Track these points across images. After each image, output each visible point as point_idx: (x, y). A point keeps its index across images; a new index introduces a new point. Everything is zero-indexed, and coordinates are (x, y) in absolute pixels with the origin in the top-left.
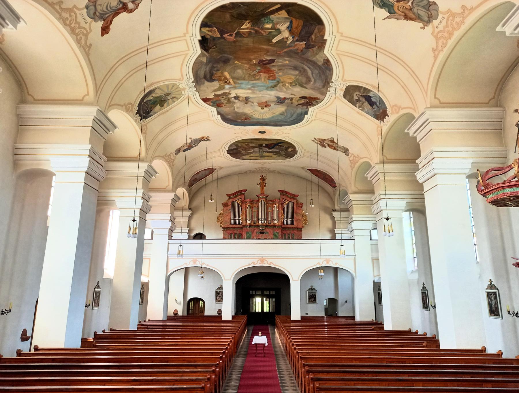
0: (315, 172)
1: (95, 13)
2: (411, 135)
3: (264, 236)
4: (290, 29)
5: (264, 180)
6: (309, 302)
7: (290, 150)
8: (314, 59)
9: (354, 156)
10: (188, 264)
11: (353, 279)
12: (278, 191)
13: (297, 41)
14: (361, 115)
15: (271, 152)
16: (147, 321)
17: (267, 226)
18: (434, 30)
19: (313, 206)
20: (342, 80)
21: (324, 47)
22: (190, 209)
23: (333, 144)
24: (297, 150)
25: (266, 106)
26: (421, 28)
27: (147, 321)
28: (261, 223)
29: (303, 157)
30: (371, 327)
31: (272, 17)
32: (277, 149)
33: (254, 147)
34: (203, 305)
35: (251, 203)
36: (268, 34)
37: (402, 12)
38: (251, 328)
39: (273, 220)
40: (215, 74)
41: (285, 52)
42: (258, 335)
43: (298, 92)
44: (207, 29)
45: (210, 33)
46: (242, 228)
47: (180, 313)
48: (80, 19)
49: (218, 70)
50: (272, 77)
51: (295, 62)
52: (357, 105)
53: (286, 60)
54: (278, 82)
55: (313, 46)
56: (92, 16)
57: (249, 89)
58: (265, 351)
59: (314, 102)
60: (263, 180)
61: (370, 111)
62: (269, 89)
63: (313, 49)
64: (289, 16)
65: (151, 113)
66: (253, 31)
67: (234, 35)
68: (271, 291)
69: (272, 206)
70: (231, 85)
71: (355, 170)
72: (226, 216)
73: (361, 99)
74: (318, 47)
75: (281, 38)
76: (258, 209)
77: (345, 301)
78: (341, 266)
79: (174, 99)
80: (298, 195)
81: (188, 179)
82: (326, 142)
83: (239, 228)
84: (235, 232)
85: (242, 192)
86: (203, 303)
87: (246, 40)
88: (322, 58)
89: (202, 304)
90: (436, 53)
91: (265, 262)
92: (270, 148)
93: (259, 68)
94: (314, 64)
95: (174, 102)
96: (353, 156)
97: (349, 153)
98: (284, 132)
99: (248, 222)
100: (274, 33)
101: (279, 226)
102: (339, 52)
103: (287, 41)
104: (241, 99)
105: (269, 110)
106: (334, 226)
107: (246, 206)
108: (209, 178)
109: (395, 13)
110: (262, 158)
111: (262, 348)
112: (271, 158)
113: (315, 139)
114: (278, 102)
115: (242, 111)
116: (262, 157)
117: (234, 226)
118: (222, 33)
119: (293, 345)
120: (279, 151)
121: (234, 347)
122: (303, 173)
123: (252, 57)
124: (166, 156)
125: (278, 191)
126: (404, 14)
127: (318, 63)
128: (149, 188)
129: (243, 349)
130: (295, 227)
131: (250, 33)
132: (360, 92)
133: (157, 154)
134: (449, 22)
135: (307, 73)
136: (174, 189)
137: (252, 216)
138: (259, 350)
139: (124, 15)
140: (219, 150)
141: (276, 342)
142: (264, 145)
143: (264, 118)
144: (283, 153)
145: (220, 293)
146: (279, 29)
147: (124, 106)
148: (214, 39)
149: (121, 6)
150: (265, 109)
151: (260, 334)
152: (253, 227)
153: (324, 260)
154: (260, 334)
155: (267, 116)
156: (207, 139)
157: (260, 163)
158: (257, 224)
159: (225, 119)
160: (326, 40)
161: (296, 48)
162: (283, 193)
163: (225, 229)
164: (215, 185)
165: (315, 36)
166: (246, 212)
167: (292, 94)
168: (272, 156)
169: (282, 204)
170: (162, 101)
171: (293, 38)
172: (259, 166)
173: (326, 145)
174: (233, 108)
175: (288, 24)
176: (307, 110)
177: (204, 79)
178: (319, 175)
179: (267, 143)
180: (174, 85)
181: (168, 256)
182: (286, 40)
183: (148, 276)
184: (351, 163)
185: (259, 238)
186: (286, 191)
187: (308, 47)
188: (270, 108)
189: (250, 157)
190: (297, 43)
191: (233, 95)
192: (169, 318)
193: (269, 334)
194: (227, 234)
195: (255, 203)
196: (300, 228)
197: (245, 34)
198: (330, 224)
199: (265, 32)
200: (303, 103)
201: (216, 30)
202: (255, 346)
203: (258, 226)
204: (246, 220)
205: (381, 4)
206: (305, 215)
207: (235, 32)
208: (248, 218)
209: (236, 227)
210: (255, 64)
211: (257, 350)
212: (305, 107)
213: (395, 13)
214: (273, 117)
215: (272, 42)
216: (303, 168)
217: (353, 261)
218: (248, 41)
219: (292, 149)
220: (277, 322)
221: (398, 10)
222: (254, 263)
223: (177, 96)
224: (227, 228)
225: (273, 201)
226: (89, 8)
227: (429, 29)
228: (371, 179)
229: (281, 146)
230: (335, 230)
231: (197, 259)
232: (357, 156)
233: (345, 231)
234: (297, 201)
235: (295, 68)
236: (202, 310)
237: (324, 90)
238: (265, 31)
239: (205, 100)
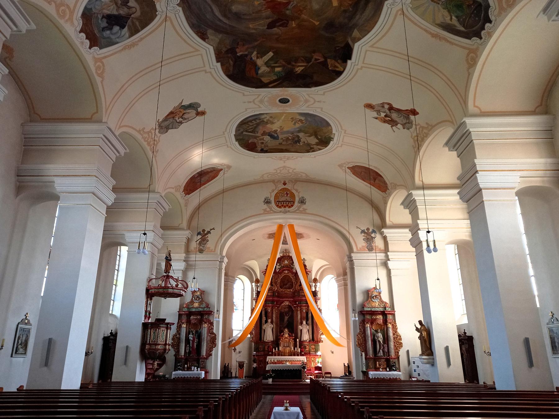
4: (256, 68)
8: (220, 36)
13: (246, 55)
21: (215, 54)
31: (275, 78)
36: (278, 61)
37: (176, 112)
41: (257, 41)
44: (337, 69)
45: (337, 64)
53: (254, 29)
55: (227, 52)
63: (227, 49)
66: (294, 64)
67: (313, 60)
74: (222, 52)
75: (264, 58)
88: (212, 40)
100: (271, 62)
103: (257, 54)
118: (325, 64)
126: (174, 112)
127: (214, 32)
131: (296, 61)
139: (395, 106)
146: (268, 67)
148: (335, 58)
165: (230, 64)
171: (251, 58)
175: (260, 72)
182: (259, 55)
187: (232, 51)
190: (246, 53)
197: (302, 60)
199: (281, 63)
201: (329, 66)
205: (192, 105)
207: (311, 63)
215: (273, 52)
221: (180, 111)
235: (238, 16)
238: (280, 65)
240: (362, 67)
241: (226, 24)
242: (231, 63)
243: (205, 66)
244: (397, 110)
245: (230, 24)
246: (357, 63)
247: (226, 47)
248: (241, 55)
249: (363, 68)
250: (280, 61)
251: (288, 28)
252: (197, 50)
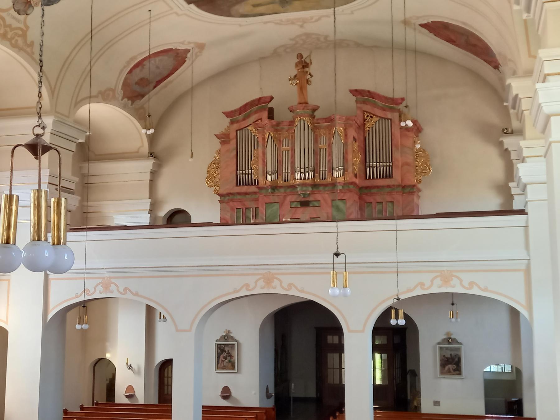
17: (315, 186)
28: (305, 179)
35: (276, 130)
60: (304, 67)
68: (336, 344)
69: (330, 133)
84: (246, 203)
101: (346, 184)
107: (264, 139)
137: (278, 163)
152: (282, 190)
158: (292, 182)
166: (264, 154)
169: (362, 127)
186: (369, 91)
195: (286, 128)
196: (409, 186)
203: (294, 187)
204: (265, 174)
224: (228, 194)
225: (330, 120)
230: (511, 184)
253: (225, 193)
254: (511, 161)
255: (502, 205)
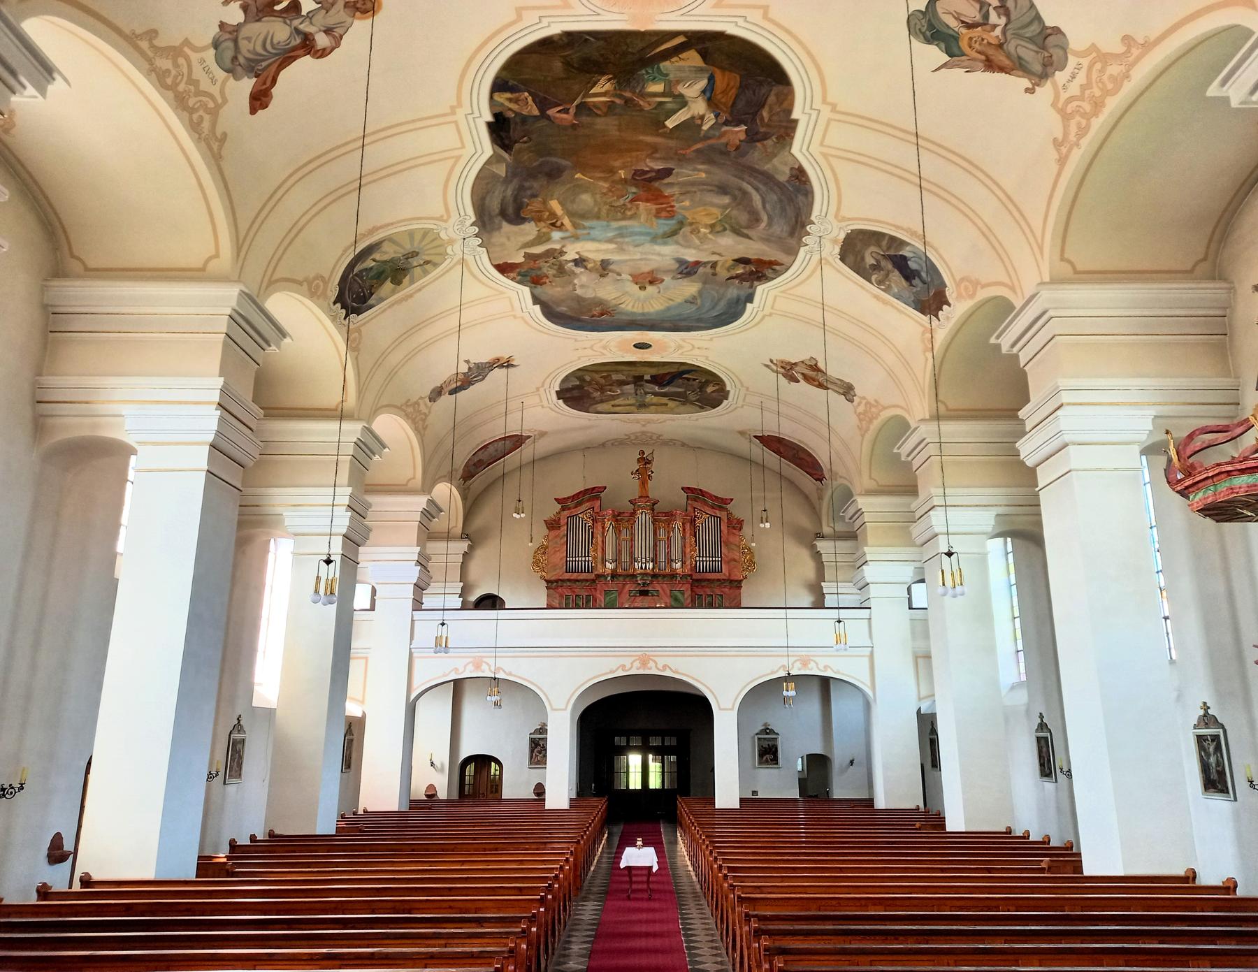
0: (773, 443)
1: (235, 58)
2: (1005, 349)
3: (647, 600)
4: (709, 93)
5: (649, 462)
6: (760, 763)
7: (710, 389)
8: (767, 167)
9: (868, 403)
10: (461, 671)
11: (868, 706)
12: (682, 489)
13: (726, 123)
14: (885, 302)
15: (664, 395)
16: (360, 812)
17: (655, 576)
18: (1057, 96)
19: (768, 525)
20: (836, 216)
21: (792, 138)
22: (465, 535)
23: (815, 373)
24: (728, 388)
25: (651, 283)
26: (1027, 90)
27: (360, 812)
28: (642, 568)
29: (742, 407)
30: (914, 825)
31: (665, 65)
32: (679, 387)
33: (621, 383)
34: (498, 773)
35: (617, 520)
36: (655, 108)
38: (618, 829)
39: (670, 561)
40: (528, 205)
42: (634, 844)
43: (729, 246)
44: (508, 95)
45: (512, 106)
46: (593, 581)
47: (442, 794)
48: (198, 73)
49: (534, 196)
50: (665, 209)
51: (720, 175)
52: (874, 278)
53: (699, 170)
54: (681, 224)
55: (766, 137)
56: (228, 63)
57: (610, 241)
58: (651, 886)
59: (769, 273)
61: (906, 294)
62: (659, 241)
63: (765, 142)
64: (706, 64)
65: (371, 301)
66: (618, 101)
67: (573, 111)
70: (567, 230)
71: (869, 436)
72: (556, 552)
73: (883, 263)
74: (777, 138)
75: (688, 116)
76: (633, 535)
77: (848, 762)
78: (838, 672)
79: (427, 267)
80: (732, 500)
81: (461, 461)
82: (797, 369)
83: (587, 580)
84: (575, 590)
85: (593, 494)
86: (498, 768)
87: (601, 123)
89: (496, 770)
90: (1064, 150)
91: (651, 664)
92: (661, 385)
93: (634, 190)
94: (768, 179)
95: (426, 273)
96: (864, 402)
97: (855, 395)
98: (696, 346)
99: (609, 566)
100: (669, 106)
101: (684, 576)
102: (825, 150)
104: (590, 266)
105: (659, 292)
106: (821, 576)
107: (603, 528)
108: (513, 458)
109: (963, 54)
110: (643, 410)
111: (645, 879)
112: (664, 408)
113: (771, 361)
114: (681, 273)
115: (593, 296)
116: (642, 406)
117: (575, 576)
118: (543, 104)
119: (720, 867)
120: (685, 392)
121: (575, 876)
122: (743, 446)
123: (617, 164)
124: (407, 406)
125: (682, 489)
126: (983, 57)
128: (366, 485)
129: (598, 882)
130: (724, 578)
131: (611, 107)
132: (880, 246)
133: (384, 401)
134: (1094, 75)
135: (751, 200)
136: (427, 488)
137: (618, 552)
138: (635, 882)
140: (538, 389)
141: (679, 863)
142: (647, 377)
143: (646, 310)
144: (692, 397)
145: (541, 743)
146: (681, 96)
147: (305, 284)
148: (524, 119)
149: (298, 41)
150: (650, 289)
151: (639, 843)
152: (621, 579)
153: (796, 658)
154: (639, 843)
155: (653, 307)
156: (507, 364)
157: (638, 422)
158: (631, 571)
159: (551, 313)
160: (796, 121)
161: (724, 140)
162: (694, 494)
163: (552, 584)
164: (527, 473)
167: (714, 253)
168: (667, 405)
169: (693, 522)
170: (397, 272)
171: (717, 116)
172: (637, 428)
173: (800, 377)
174: (571, 288)
175: (703, 83)
176: (751, 291)
177: (500, 218)
178: (782, 450)
179: (654, 371)
180: (426, 233)
181: (413, 650)
183: (363, 702)
184: (860, 420)
185: (636, 605)
187: (753, 137)
188: (661, 286)
189: (613, 406)
190: (725, 128)
191: (571, 254)
192: (415, 805)
193: (662, 843)
194: (557, 595)
196: (736, 581)
197: (599, 109)
198: (809, 570)
200: (742, 274)
201: (530, 99)
202: (626, 872)
203: (633, 576)
204: (604, 561)
205: (928, 34)
206: (749, 549)
207: (575, 103)
208: (609, 556)
209: (579, 578)
210: (625, 181)
211: (631, 882)
212: (746, 284)
213: (963, 54)
214: (668, 309)
215: (665, 126)
216: (742, 433)
217: (866, 661)
218: (607, 126)
219: (717, 387)
220: (681, 813)
221: (970, 47)
222: (623, 666)
223: (435, 259)
224: (557, 581)
225: (670, 515)
226: (220, 48)
227: (1045, 92)
228: (910, 458)
229: (688, 379)
230: (823, 584)
231: (485, 660)
232: (873, 402)
233: (845, 588)
234: (729, 514)
235: (723, 189)
236: (496, 785)
237: (793, 242)
238: (649, 99)
239: (504, 269)
240: (453, 113)
241: (748, 183)
242: (765, 113)
243: (829, 121)
244: (292, 54)
245: (740, 181)
246: (470, 117)
247: (764, 145)
248: (737, 125)
249: (448, 111)
250: (651, 108)
251: (633, 168)
252: (825, 155)
253: (553, 578)
254: (822, 562)
255: (813, 603)
